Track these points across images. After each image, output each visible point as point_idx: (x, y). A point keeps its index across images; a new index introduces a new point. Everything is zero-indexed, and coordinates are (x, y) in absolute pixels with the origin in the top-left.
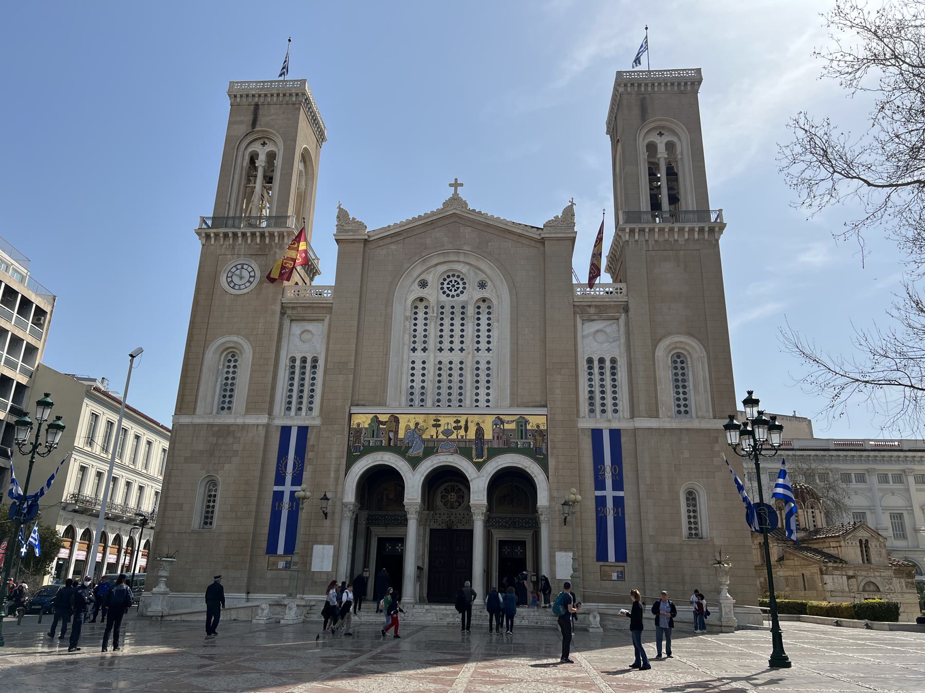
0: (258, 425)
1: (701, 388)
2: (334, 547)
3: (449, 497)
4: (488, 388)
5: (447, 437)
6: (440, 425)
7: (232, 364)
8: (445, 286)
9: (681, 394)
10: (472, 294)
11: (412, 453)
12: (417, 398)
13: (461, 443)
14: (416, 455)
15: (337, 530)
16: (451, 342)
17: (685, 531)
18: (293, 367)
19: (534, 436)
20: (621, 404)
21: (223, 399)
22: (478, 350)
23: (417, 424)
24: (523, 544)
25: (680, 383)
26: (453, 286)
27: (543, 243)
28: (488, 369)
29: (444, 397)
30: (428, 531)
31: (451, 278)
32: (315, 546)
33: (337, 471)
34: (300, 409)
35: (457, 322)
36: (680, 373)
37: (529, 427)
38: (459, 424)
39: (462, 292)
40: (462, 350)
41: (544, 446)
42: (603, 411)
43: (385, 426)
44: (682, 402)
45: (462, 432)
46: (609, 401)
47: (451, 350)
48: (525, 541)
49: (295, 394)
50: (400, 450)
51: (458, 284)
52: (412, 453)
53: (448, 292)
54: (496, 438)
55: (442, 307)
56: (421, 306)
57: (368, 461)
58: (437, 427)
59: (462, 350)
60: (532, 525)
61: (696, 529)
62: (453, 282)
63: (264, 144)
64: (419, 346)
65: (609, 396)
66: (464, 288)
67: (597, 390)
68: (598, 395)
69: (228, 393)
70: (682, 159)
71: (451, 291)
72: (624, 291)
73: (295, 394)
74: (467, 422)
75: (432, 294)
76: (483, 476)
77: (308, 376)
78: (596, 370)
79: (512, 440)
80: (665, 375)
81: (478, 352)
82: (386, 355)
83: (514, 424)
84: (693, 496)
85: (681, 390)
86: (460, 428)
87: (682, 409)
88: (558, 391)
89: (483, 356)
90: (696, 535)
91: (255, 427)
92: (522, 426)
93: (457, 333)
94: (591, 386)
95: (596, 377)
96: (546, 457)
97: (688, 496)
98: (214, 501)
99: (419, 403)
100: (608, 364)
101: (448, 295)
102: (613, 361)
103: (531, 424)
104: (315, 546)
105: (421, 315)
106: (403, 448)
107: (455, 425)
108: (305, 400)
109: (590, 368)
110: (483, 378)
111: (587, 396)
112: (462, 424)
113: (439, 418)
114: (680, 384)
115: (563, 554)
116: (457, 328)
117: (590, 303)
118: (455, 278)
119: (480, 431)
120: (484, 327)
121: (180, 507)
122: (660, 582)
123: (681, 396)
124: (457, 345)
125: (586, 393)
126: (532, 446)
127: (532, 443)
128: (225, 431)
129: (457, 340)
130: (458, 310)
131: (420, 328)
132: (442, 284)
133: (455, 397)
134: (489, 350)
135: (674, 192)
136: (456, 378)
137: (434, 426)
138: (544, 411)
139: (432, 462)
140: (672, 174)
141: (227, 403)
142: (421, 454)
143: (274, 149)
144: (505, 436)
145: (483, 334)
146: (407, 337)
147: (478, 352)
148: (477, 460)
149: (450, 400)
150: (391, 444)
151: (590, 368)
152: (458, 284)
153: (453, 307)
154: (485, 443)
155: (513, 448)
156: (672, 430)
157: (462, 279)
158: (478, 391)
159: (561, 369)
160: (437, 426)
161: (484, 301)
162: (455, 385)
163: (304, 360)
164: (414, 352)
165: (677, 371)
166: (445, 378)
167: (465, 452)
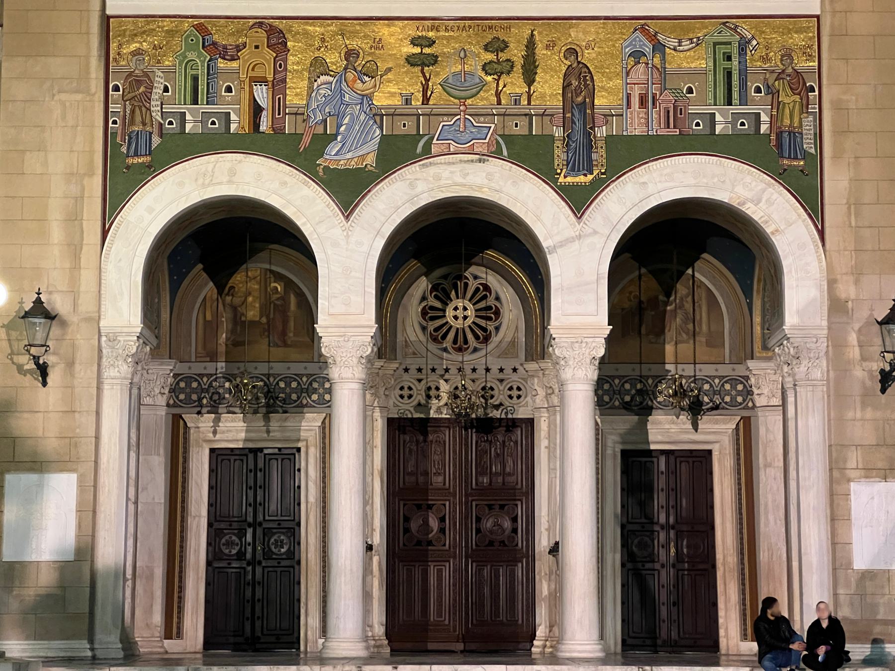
2: (81, 487)
3: (450, 313)
6: (434, 60)
13: (510, 122)
14: (353, 165)
15: (87, 422)
19: (772, 92)
23: (351, 55)
30: (380, 425)
32: (9, 478)
33: (73, 218)
38: (503, 56)
41: (808, 125)
43: (235, 64)
45: (514, 84)
57: (181, 184)
58: (423, 65)
60: (733, 399)
74: (531, 45)
76: (595, 232)
79: (692, 109)
83: (701, 50)
92: (729, 58)
96: (815, 162)
104: (9, 478)
106: (306, 140)
107: (490, 57)
112: (516, 53)
113: (431, 34)
126: (764, 128)
127: (764, 118)
137: (411, 61)
139: (412, 186)
142: (371, 160)
144: (668, 96)
148: (569, 179)
150: (263, 128)
154: (599, 120)
155: (696, 136)
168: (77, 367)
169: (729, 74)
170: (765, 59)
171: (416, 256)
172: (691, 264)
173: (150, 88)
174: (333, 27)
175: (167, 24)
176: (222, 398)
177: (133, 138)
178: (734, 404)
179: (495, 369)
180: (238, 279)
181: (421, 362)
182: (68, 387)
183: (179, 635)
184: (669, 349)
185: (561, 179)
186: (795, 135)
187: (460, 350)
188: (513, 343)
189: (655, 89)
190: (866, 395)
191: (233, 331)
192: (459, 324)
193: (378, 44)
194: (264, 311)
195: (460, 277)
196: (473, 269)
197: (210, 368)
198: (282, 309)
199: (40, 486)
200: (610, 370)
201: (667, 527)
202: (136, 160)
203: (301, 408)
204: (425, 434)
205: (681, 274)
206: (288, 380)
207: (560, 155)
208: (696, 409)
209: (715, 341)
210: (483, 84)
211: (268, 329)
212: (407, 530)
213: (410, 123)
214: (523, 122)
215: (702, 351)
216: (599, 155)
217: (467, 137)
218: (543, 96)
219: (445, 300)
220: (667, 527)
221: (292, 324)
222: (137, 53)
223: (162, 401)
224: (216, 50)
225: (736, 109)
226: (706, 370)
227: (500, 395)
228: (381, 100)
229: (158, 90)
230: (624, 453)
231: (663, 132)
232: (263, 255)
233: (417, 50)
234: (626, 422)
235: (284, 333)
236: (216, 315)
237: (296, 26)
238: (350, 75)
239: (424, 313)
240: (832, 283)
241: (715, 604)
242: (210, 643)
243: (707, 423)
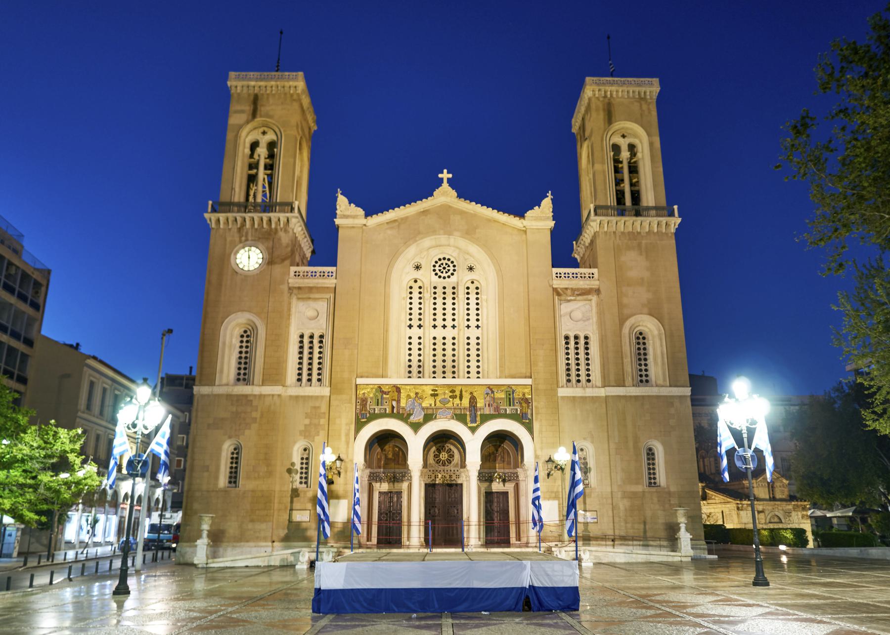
0: (273, 395)
1: (659, 360)
3: (441, 456)
4: (478, 361)
5: (444, 405)
6: (437, 395)
7: (245, 339)
8: (437, 268)
9: (643, 366)
10: (462, 278)
11: (413, 419)
12: (415, 369)
13: (456, 411)
14: (417, 421)
16: (444, 320)
17: (646, 481)
18: (301, 342)
19: (521, 403)
20: (594, 374)
21: (238, 371)
22: (468, 327)
23: (417, 394)
24: (505, 494)
25: (641, 355)
26: (444, 268)
27: (525, 232)
28: (478, 344)
29: (439, 370)
31: (442, 261)
33: (347, 435)
34: (309, 380)
35: (449, 301)
36: (642, 348)
37: (516, 396)
38: (454, 394)
39: (452, 274)
40: (454, 327)
41: (529, 411)
42: (579, 381)
43: (388, 396)
44: (644, 373)
45: (457, 401)
46: (583, 372)
47: (444, 327)
48: (508, 492)
49: (305, 367)
50: (404, 417)
51: (449, 266)
52: (413, 419)
53: (440, 274)
54: (487, 405)
55: (435, 288)
56: (416, 286)
59: (454, 327)
61: (655, 478)
62: (444, 264)
63: (264, 133)
64: (415, 323)
65: (583, 367)
66: (454, 270)
67: (572, 362)
68: (573, 367)
69: (243, 366)
70: (643, 158)
71: (442, 272)
72: (596, 276)
73: (305, 367)
74: (461, 391)
75: (427, 277)
77: (316, 350)
78: (572, 345)
79: (501, 407)
80: (628, 348)
81: (468, 328)
82: (387, 331)
83: (503, 393)
84: (652, 452)
85: (643, 362)
86: (455, 397)
87: (644, 378)
88: (541, 364)
89: (473, 333)
90: (655, 483)
91: (271, 397)
92: (510, 395)
93: (449, 311)
94: (568, 359)
95: (572, 351)
97: (648, 451)
98: (236, 463)
99: (417, 375)
100: (582, 341)
101: (440, 277)
102: (586, 338)
103: (518, 393)
105: (416, 295)
106: (405, 415)
107: (451, 394)
108: (315, 372)
109: (567, 343)
110: (473, 352)
111: (564, 367)
112: (458, 393)
114: (642, 357)
115: (551, 502)
116: (449, 306)
117: (566, 287)
118: (446, 261)
119: (473, 400)
120: (473, 306)
121: (206, 468)
122: (626, 523)
123: (643, 367)
124: (449, 323)
125: (564, 365)
126: (519, 412)
127: (519, 410)
128: (245, 399)
129: (449, 317)
130: (449, 291)
131: (415, 306)
132: (434, 266)
133: (449, 369)
134: (478, 327)
135: (636, 188)
136: (449, 352)
137: (432, 395)
138: (529, 381)
140: (634, 169)
141: (242, 375)
142: (421, 420)
143: (274, 138)
145: (473, 312)
146: (403, 315)
147: (468, 328)
149: (444, 372)
150: (395, 411)
151: (567, 343)
152: (449, 266)
153: (444, 288)
154: (478, 410)
156: (636, 397)
157: (452, 262)
158: (469, 364)
159: (543, 345)
160: (434, 395)
161: (473, 282)
162: (449, 358)
163: (312, 337)
164: (410, 328)
165: (639, 346)
166: (439, 352)
167: (461, 418)
168: (348, 473)
169: (510, 399)
170: (519, 395)
171: (433, 441)
172: (503, 442)
173: (367, 402)
174: (412, 387)
175: (371, 386)
176: (382, 478)
177: (362, 415)
178: (514, 479)
179: (452, 470)
180: (387, 447)
181: (434, 469)
182: (346, 478)
183: (371, 541)
184: (497, 465)
185: (469, 425)
186: (526, 414)
187: (444, 466)
188: (457, 464)
189: (492, 402)
190: (544, 479)
191: (385, 461)
192: (443, 459)
193: (423, 391)
194: (393, 455)
195: (444, 447)
196: (447, 445)
197: (379, 470)
198: (398, 455)
199: (338, 503)
200: (482, 471)
201: (497, 512)
202: (363, 420)
203: (402, 481)
204: (435, 488)
205: (500, 446)
206: (399, 474)
207: (468, 419)
208: (504, 481)
209: (509, 463)
210: (449, 401)
211: (394, 460)
212: (430, 513)
213: (431, 411)
214: (460, 410)
215: (505, 465)
216: (478, 419)
217: (444, 414)
218: (464, 404)
219: (440, 453)
220: (497, 512)
221: (400, 459)
222: (364, 394)
223: (367, 479)
224: (383, 392)
225: (512, 407)
226: (507, 471)
227: (454, 477)
228: (424, 405)
229: (368, 403)
230: (486, 492)
231: (494, 413)
232: (393, 441)
233: (433, 392)
234: (486, 484)
235: (398, 461)
236: (381, 457)
237: (403, 386)
238: (417, 399)
239: (434, 456)
240: (535, 451)
241: (509, 532)
242: (378, 543)
243: (507, 484)
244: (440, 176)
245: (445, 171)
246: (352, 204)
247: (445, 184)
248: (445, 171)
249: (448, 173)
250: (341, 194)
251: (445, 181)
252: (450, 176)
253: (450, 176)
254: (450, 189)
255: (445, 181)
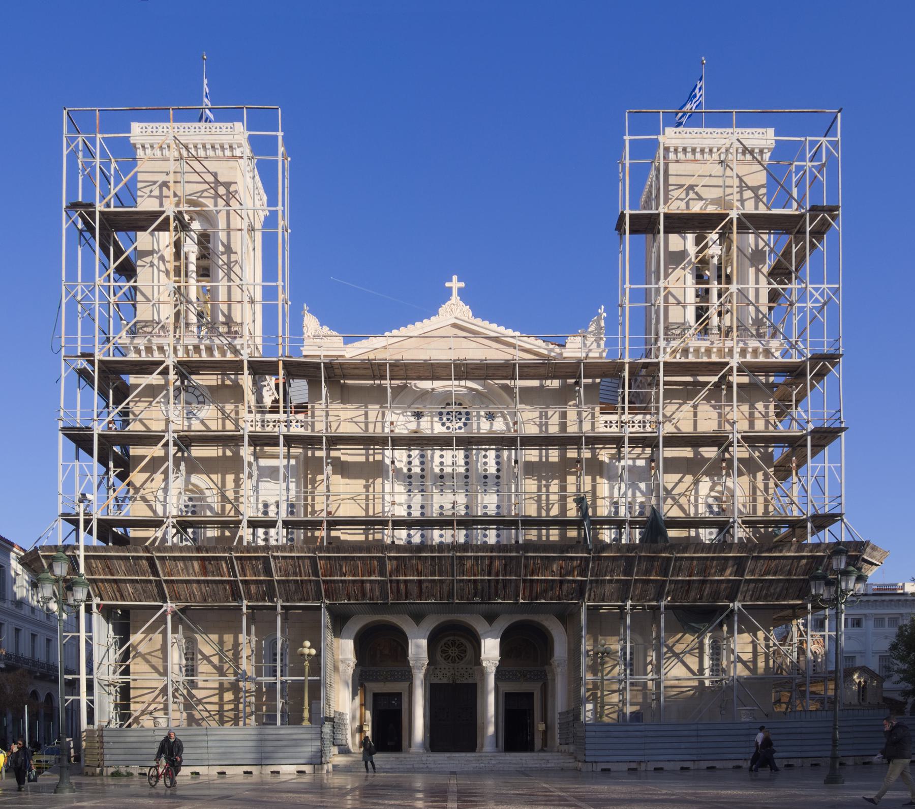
3: (450, 651)
24: (530, 696)
187: (453, 662)
244: (447, 284)
245: (455, 278)
246: (325, 327)
247: (455, 298)
248: (455, 278)
249: (459, 281)
250: (309, 312)
251: (455, 292)
252: (462, 285)
253: (462, 285)
254: (461, 303)
255: (455, 292)
